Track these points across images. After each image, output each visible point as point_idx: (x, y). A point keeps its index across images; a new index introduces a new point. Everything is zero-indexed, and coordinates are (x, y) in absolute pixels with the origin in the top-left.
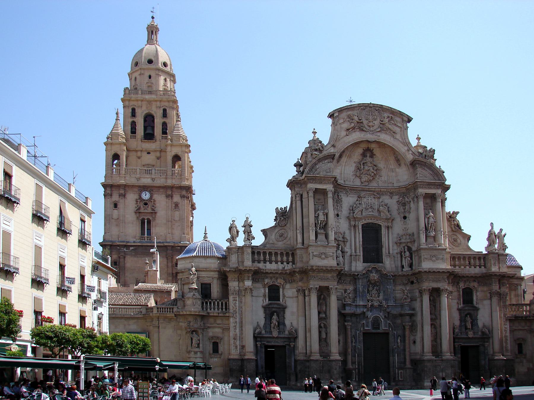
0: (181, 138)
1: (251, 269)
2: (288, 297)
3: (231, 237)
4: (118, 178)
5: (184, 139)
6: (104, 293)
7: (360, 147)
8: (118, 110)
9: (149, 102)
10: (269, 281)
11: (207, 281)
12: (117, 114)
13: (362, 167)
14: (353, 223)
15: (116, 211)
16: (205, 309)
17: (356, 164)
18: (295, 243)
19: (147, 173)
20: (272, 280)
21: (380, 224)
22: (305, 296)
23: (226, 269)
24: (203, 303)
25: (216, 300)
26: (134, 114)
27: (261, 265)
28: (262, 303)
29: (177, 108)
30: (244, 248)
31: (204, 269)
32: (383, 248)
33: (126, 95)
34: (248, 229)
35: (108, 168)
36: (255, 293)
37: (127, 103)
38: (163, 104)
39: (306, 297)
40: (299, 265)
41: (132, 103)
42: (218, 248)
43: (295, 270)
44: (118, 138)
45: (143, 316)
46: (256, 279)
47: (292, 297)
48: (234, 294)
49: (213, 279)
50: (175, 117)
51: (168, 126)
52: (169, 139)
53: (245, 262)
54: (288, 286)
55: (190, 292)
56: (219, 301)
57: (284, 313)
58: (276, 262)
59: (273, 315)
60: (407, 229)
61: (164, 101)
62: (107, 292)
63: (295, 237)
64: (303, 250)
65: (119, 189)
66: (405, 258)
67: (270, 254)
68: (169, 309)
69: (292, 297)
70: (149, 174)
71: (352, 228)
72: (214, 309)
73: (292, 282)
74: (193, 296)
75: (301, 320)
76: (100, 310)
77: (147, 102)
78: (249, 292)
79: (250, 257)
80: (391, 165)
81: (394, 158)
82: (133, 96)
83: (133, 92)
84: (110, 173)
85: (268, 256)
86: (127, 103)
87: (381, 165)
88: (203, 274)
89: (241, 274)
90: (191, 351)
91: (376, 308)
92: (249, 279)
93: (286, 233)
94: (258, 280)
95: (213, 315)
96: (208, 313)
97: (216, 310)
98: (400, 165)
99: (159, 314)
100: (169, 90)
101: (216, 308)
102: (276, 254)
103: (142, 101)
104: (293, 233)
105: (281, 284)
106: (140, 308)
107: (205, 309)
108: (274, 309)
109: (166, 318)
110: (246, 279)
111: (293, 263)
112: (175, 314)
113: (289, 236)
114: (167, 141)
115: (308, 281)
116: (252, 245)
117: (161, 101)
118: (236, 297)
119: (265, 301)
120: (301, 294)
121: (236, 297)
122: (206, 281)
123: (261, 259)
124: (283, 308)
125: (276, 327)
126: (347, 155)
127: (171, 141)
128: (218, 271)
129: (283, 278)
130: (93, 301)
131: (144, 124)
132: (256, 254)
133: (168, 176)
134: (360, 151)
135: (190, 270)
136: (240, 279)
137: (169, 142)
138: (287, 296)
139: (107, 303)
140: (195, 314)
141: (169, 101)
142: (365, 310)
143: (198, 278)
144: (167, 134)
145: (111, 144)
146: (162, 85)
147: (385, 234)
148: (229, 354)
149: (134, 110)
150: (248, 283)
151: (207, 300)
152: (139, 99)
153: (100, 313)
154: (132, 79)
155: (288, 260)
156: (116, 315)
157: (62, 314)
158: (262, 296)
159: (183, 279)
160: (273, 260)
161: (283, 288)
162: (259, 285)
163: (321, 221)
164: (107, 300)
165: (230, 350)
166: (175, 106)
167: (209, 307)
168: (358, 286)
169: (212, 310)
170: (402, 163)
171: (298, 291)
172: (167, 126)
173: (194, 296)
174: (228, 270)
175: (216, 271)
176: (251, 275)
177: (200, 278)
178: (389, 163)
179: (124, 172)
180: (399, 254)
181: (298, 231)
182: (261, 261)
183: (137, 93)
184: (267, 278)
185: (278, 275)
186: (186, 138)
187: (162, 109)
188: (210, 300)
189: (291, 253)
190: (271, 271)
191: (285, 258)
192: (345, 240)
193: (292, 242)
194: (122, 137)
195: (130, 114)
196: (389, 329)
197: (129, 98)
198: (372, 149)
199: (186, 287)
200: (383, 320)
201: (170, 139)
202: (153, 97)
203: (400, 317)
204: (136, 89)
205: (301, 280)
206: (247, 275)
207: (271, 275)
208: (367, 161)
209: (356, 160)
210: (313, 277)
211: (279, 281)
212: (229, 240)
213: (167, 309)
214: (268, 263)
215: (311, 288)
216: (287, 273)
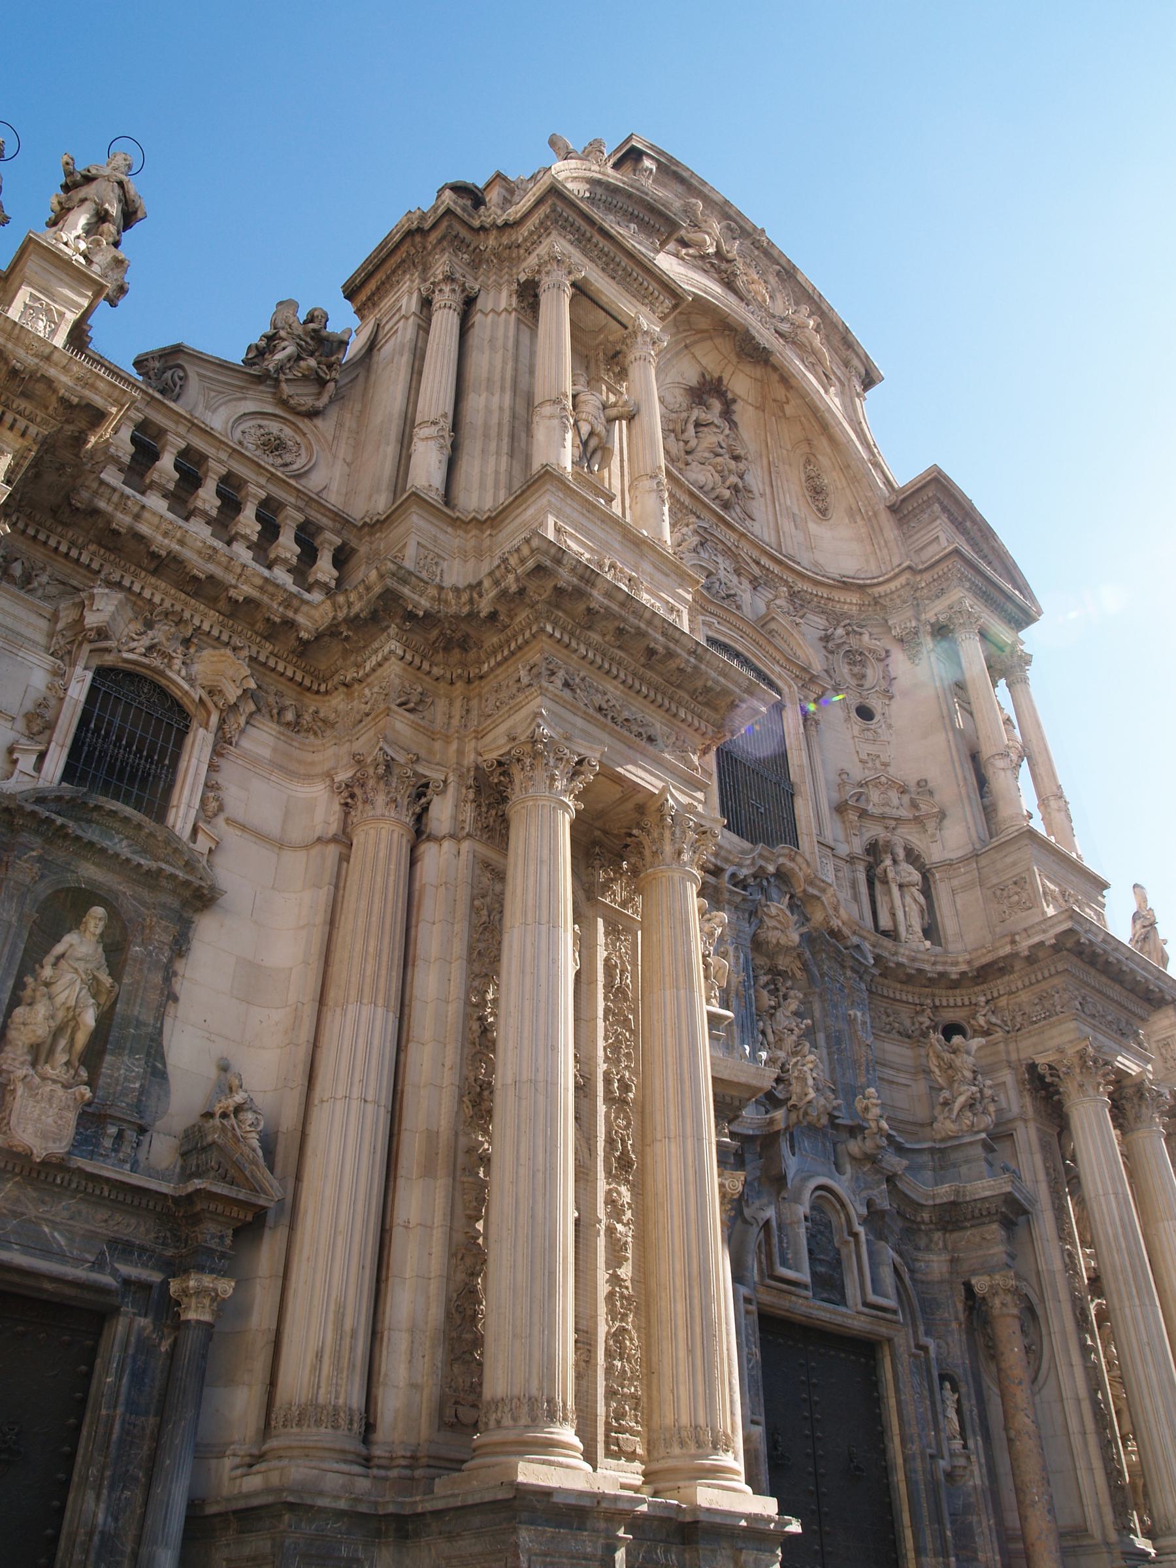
1: (52, 372)
2: (243, 827)
10: (127, 627)
13: (691, 430)
32: (799, 803)
59: (77, 922)
60: (885, 765)
69: (280, 845)
87: (755, 480)
93: (303, 451)
98: (823, 512)
108: (90, 872)
119: (26, 762)
125: (61, 1058)
160: (199, 504)
161: (222, 743)
170: (839, 503)
178: (786, 487)
200: (861, 1230)
203: (937, 1235)
207: (159, 592)
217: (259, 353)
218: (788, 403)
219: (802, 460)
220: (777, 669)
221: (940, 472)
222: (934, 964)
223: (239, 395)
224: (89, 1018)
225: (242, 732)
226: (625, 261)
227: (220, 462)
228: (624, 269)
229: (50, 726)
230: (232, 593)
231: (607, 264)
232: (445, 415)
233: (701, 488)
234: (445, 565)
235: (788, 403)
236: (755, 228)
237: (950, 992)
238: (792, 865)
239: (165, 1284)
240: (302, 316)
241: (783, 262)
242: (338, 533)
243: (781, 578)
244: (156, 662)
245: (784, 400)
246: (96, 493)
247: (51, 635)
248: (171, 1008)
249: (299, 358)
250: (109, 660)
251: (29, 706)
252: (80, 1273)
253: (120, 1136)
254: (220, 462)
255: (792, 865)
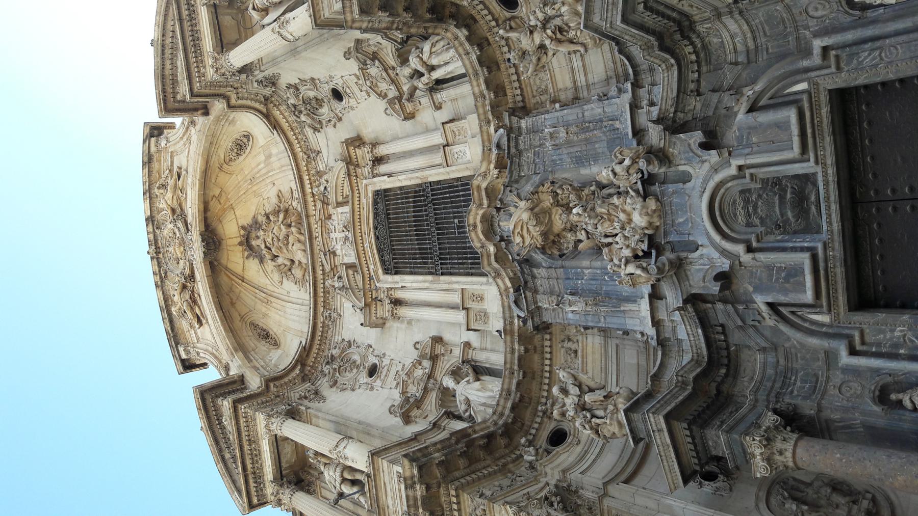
7: (244, 269)
14: (385, 309)
17: (285, 280)
21: (370, 195)
32: (431, 179)
66: (432, 68)
71: (402, 311)
80: (259, 164)
81: (241, 158)
91: (662, 212)
126: (264, 310)
134: (253, 270)
142: (672, 297)
147: (390, 175)
163: (344, 480)
168: (570, 315)
178: (256, 170)
180: (439, 96)
192: (428, 350)
196: (793, 101)
198: (242, 232)
208: (263, 246)
209: (276, 276)
218: (214, 196)
219: (232, 163)
220: (364, 201)
221: (160, 111)
222: (468, 54)
226: (246, 448)
228: (250, 445)
231: (256, 455)
233: (304, 251)
235: (214, 196)
236: (152, 258)
237: (478, 17)
238: (478, 224)
241: (150, 229)
243: (308, 170)
245: (214, 199)
255: (478, 224)
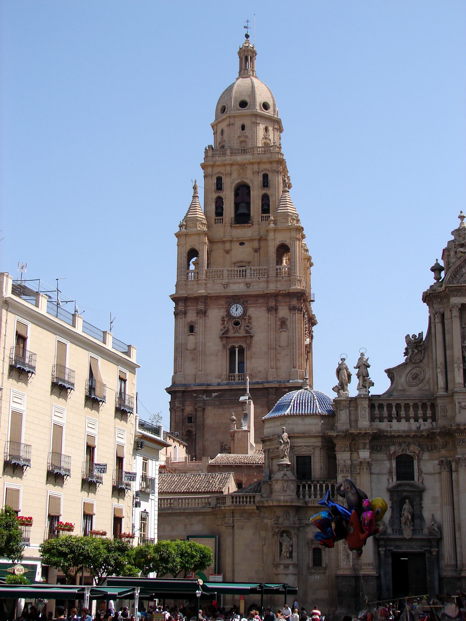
0: (289, 218)
1: (367, 431)
3: (340, 384)
4: (196, 286)
5: (293, 219)
6: (153, 480)
8: (195, 182)
9: (243, 166)
10: (397, 448)
11: (305, 453)
12: (195, 188)
15: (192, 338)
16: (301, 497)
18: (436, 387)
19: (239, 275)
20: (402, 447)
22: (451, 471)
23: (332, 434)
24: (298, 487)
25: (318, 482)
26: (219, 186)
27: (384, 425)
28: (387, 484)
29: (285, 171)
30: (358, 400)
31: (300, 433)
33: (208, 158)
34: (364, 371)
35: (181, 272)
36: (375, 469)
37: (209, 170)
38: (263, 167)
39: (453, 474)
40: (441, 422)
41: (216, 170)
42: (322, 399)
43: (434, 431)
44: (196, 225)
45: (211, 510)
46: (377, 447)
47: (434, 474)
48: (345, 472)
49: (314, 449)
50: (281, 185)
51: (270, 200)
52: (272, 220)
53: (359, 422)
54: (426, 456)
55: (279, 470)
56: (322, 482)
57: (421, 499)
58: (408, 420)
59: (404, 503)
61: (263, 163)
62: (157, 477)
63: (435, 379)
64: (446, 398)
65: (198, 303)
67: (398, 406)
68: (245, 498)
69: (434, 474)
70: (241, 277)
72: (315, 496)
73: (431, 449)
74: (283, 477)
75: (447, 510)
76: (144, 505)
77: (238, 166)
78: (365, 469)
79: (367, 413)
82: (219, 160)
83: (218, 152)
84: (184, 279)
85: (394, 411)
86: (209, 170)
88: (299, 442)
89: (353, 440)
90: (280, 564)
92: (364, 448)
93: (423, 373)
94: (381, 449)
95: (312, 505)
96: (306, 503)
97: (318, 496)
99: (234, 506)
100: (273, 144)
101: (318, 494)
102: (407, 406)
103: (231, 165)
104: (433, 372)
105: (415, 453)
106: (208, 498)
107: (301, 497)
108: (405, 494)
109: (244, 511)
110: (361, 447)
111: (434, 419)
112: (257, 507)
113: (427, 377)
114: (269, 224)
115: (455, 448)
116: (370, 395)
117: (259, 163)
118: (348, 477)
119: (391, 481)
120: (444, 468)
121: (348, 477)
122: (304, 452)
123: (384, 416)
124: (420, 492)
127: (275, 222)
128: (322, 437)
129: (417, 444)
130: (135, 493)
131: (235, 200)
132: (377, 408)
133: (270, 278)
135: (280, 437)
136: (353, 449)
137: (272, 225)
138: (424, 469)
139: (156, 494)
140: (285, 504)
141: (271, 162)
143: (292, 448)
144: (269, 213)
145: (186, 234)
146: (261, 139)
148: (338, 567)
149: (219, 180)
150: (364, 454)
151: (304, 483)
152: (227, 162)
153: (143, 510)
154: (216, 132)
155: (425, 414)
156: (172, 509)
157: (88, 517)
158: (387, 472)
159: (271, 450)
161: (419, 460)
162: (381, 456)
164: (157, 490)
165: (338, 559)
166: (281, 169)
167: (307, 492)
169: (313, 497)
171: (441, 463)
172: (269, 200)
173: (285, 478)
174: (335, 434)
175: (318, 436)
176: (368, 441)
177: (296, 449)
179: (204, 276)
181: (439, 370)
182: (384, 418)
183: (224, 154)
184: (393, 445)
185: (409, 440)
186: (297, 217)
187: (261, 175)
188: (309, 483)
189: (430, 403)
190: (399, 434)
191: (420, 412)
193: (432, 385)
194: (203, 224)
195: (214, 187)
197: (212, 163)
199: (275, 462)
201: (273, 221)
202: (248, 157)
204: (223, 147)
205: (444, 446)
206: (362, 441)
207: (400, 440)
210: (461, 442)
211: (412, 448)
212: (337, 388)
213: (246, 498)
214: (395, 421)
215: (459, 459)
216: (423, 435)
217: (406, 354)
223: (405, 369)
224: (410, 517)
225: (422, 456)
227: (403, 403)
229: (392, 472)
230: (411, 436)
232: (441, 363)
234: (447, 407)
239: (430, 550)
240: (411, 337)
242: (429, 402)
244: (404, 452)
246: (383, 433)
247: (387, 457)
248: (423, 509)
249: (413, 351)
250: (397, 455)
251: (388, 470)
252: (419, 550)
253: (419, 532)
254: (403, 403)
